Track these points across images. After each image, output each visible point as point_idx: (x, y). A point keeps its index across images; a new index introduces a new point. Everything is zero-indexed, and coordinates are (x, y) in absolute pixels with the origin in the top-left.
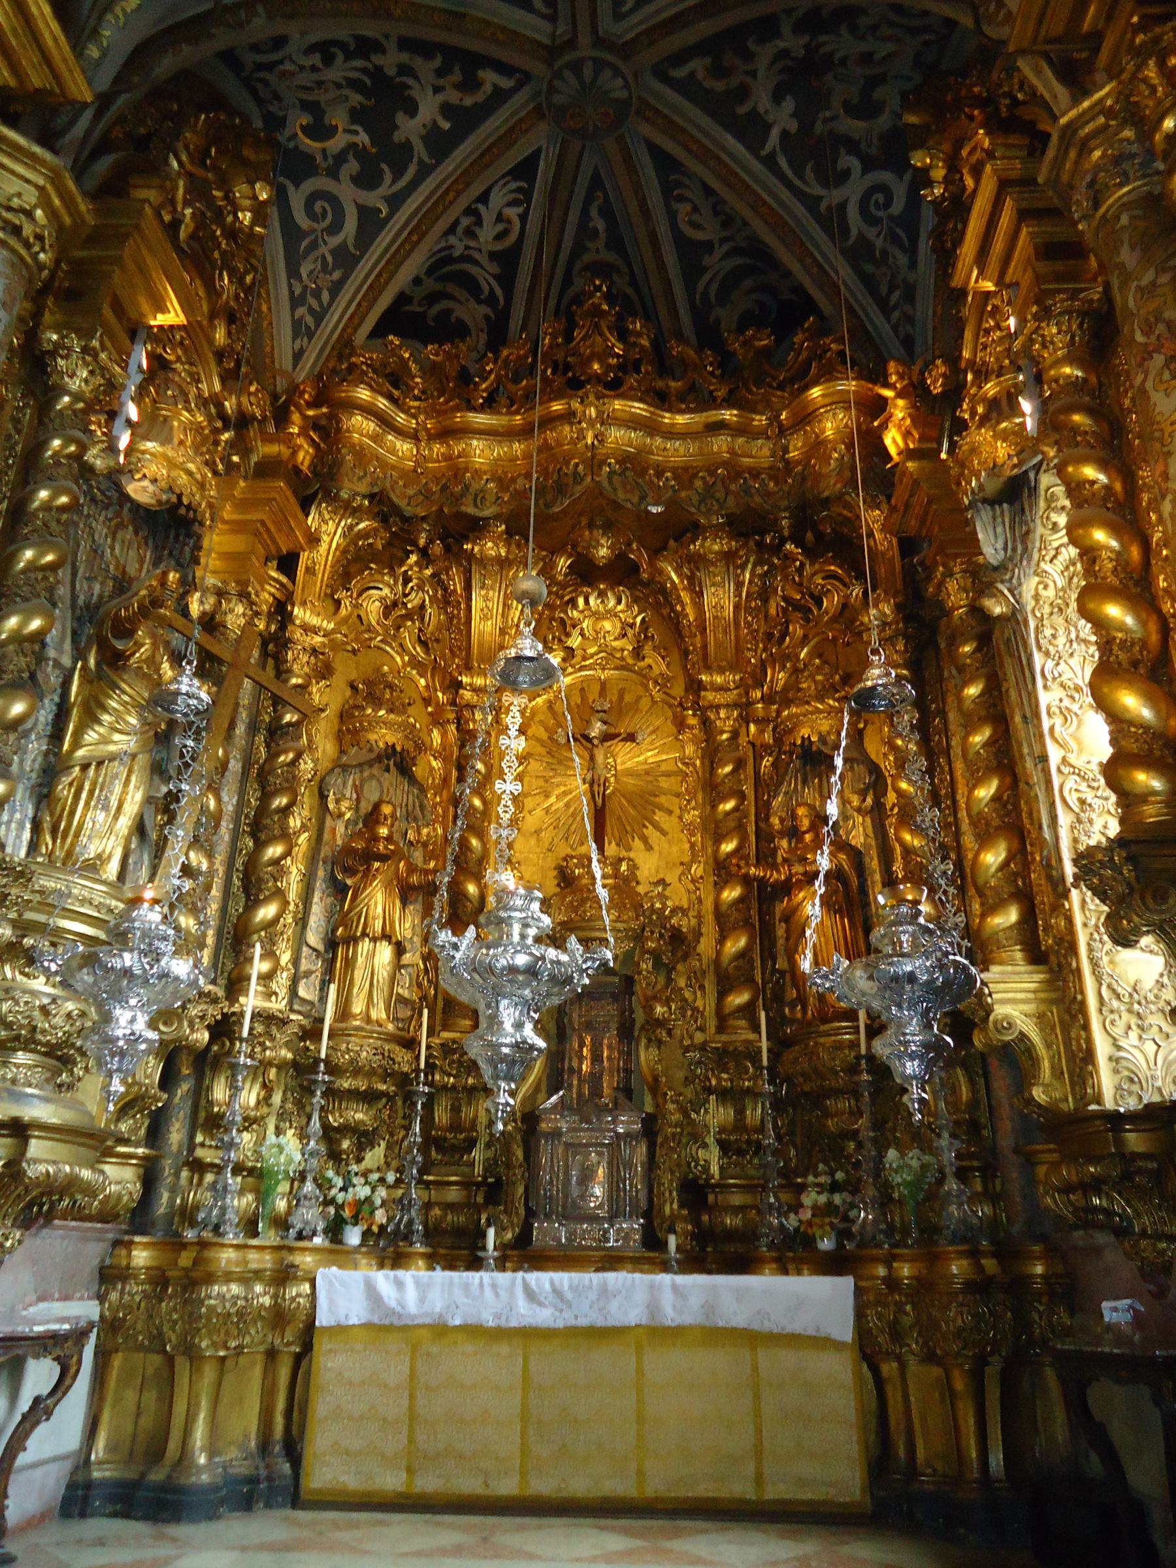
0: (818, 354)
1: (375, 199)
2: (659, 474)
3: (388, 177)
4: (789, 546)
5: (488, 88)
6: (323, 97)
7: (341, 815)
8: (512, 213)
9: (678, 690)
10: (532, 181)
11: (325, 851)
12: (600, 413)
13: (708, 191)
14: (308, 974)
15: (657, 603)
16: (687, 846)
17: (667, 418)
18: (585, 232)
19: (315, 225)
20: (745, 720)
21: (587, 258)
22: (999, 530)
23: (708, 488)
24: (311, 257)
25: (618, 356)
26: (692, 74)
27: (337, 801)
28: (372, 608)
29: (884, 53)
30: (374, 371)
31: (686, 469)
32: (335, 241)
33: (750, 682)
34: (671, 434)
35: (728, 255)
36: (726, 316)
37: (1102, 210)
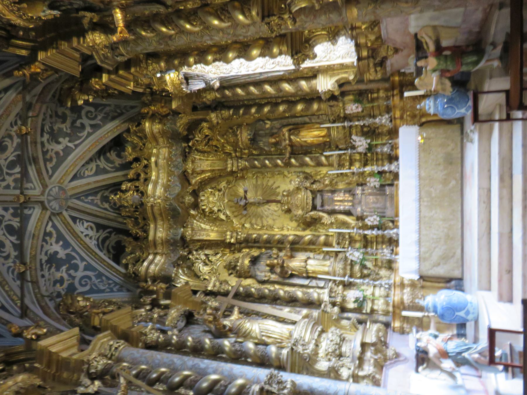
0: (135, 133)
1: (82, 265)
2: (170, 181)
3: (75, 261)
4: (190, 144)
5: (52, 229)
6: (52, 280)
7: (269, 276)
8: (86, 224)
9: (231, 178)
10: (77, 218)
11: (280, 280)
12: (152, 197)
13: (83, 165)
14: (317, 284)
15: (204, 184)
16: (278, 176)
17: (153, 178)
18: (92, 203)
19: (89, 284)
20: (241, 158)
21: (99, 203)
22: (196, 83)
23: (174, 166)
24: (99, 286)
25: (133, 192)
26: (51, 168)
27: (265, 276)
28: (205, 269)
29: (50, 112)
30: (135, 266)
31: (168, 173)
32: (94, 278)
33: (230, 157)
34: (158, 177)
35: (100, 161)
36: (118, 162)
37: (125, 54)
